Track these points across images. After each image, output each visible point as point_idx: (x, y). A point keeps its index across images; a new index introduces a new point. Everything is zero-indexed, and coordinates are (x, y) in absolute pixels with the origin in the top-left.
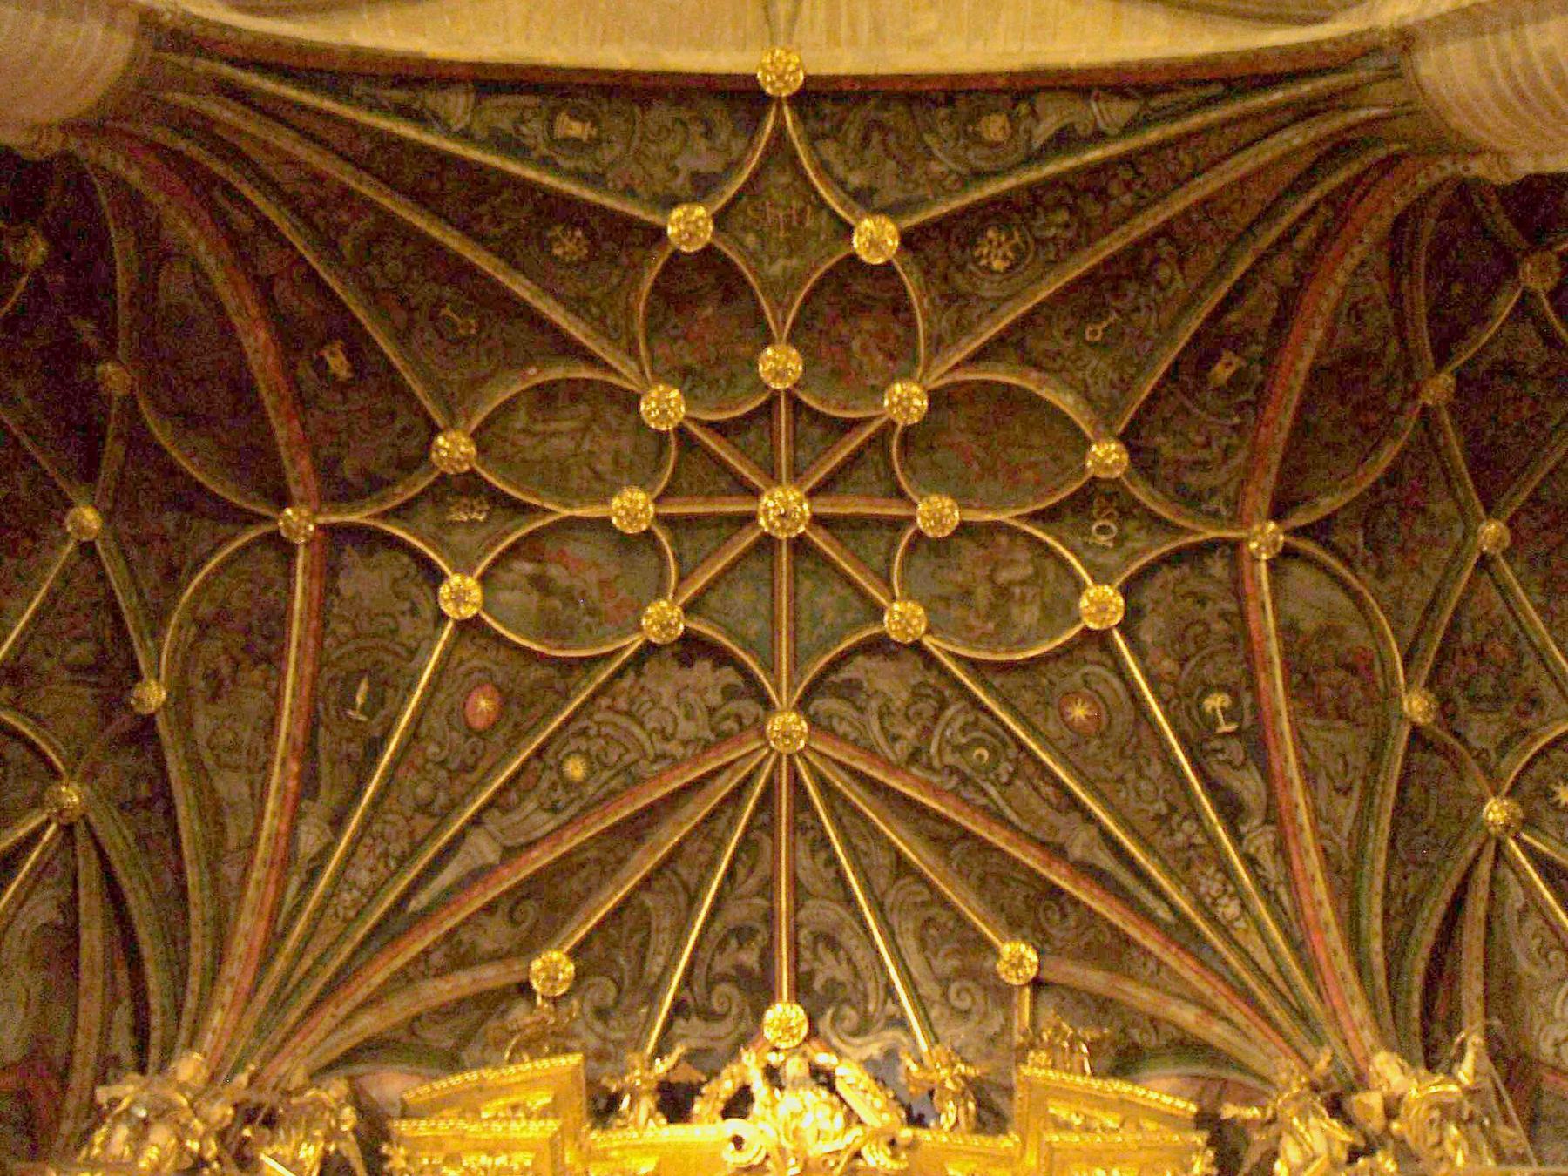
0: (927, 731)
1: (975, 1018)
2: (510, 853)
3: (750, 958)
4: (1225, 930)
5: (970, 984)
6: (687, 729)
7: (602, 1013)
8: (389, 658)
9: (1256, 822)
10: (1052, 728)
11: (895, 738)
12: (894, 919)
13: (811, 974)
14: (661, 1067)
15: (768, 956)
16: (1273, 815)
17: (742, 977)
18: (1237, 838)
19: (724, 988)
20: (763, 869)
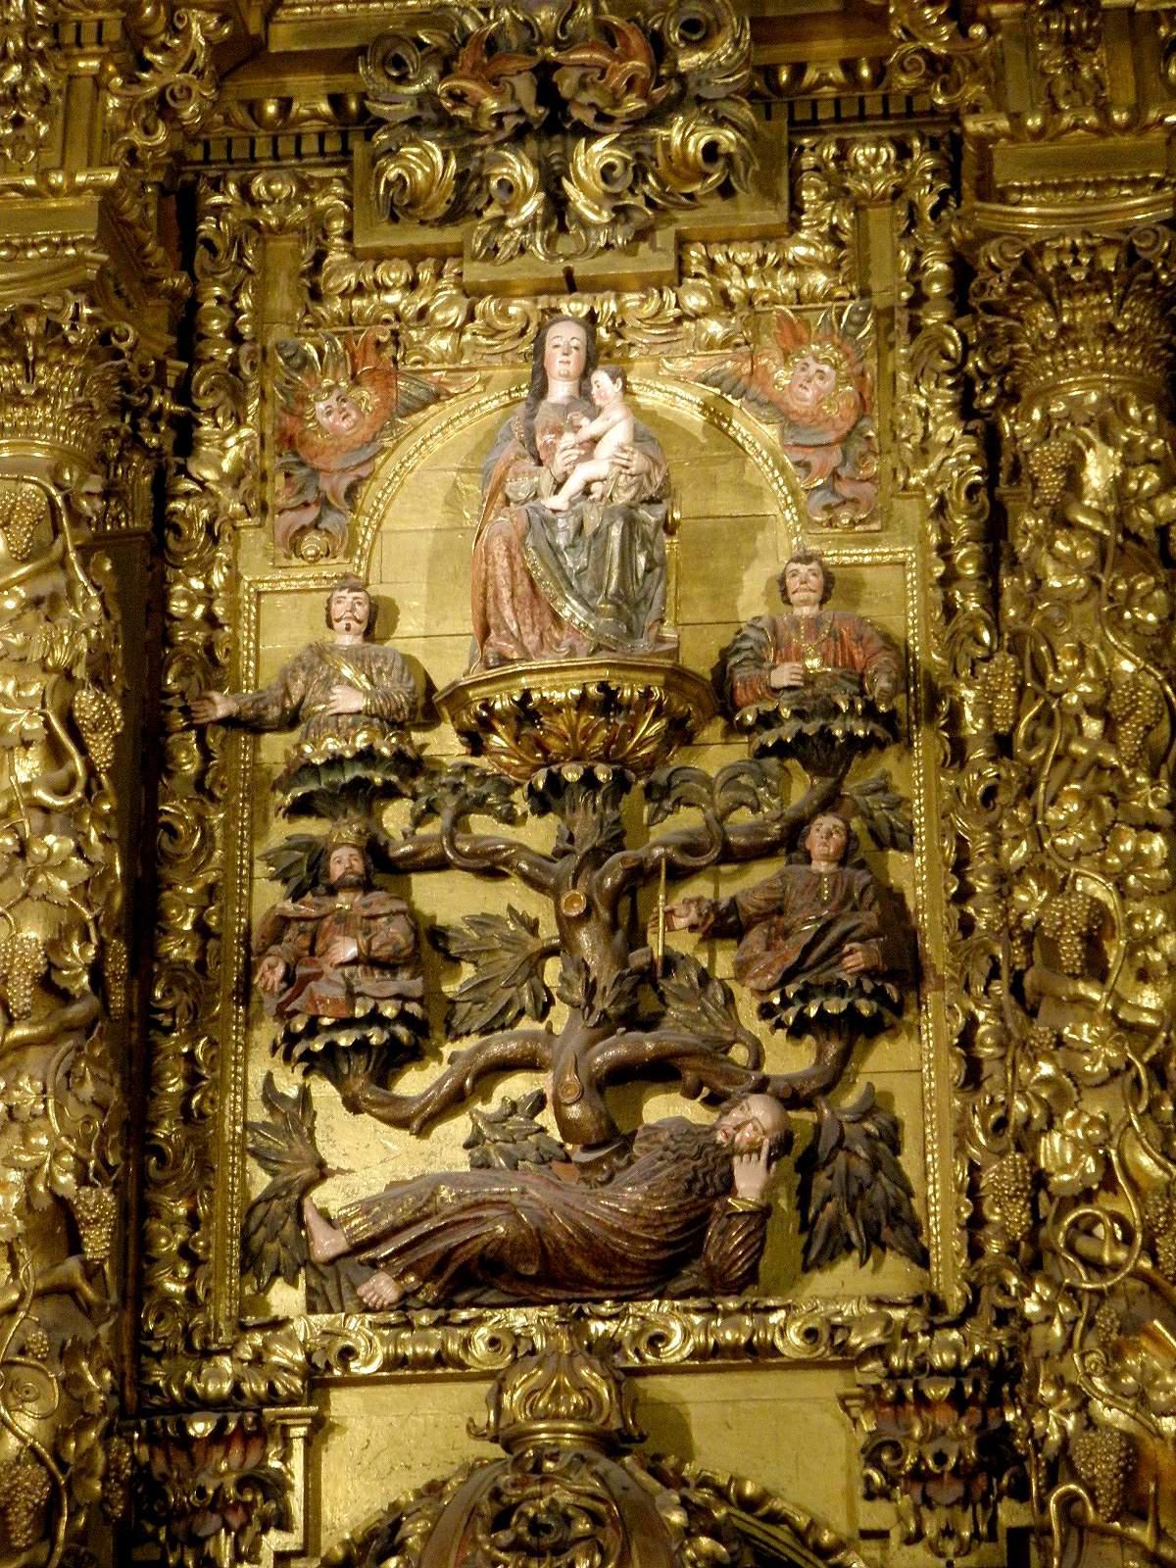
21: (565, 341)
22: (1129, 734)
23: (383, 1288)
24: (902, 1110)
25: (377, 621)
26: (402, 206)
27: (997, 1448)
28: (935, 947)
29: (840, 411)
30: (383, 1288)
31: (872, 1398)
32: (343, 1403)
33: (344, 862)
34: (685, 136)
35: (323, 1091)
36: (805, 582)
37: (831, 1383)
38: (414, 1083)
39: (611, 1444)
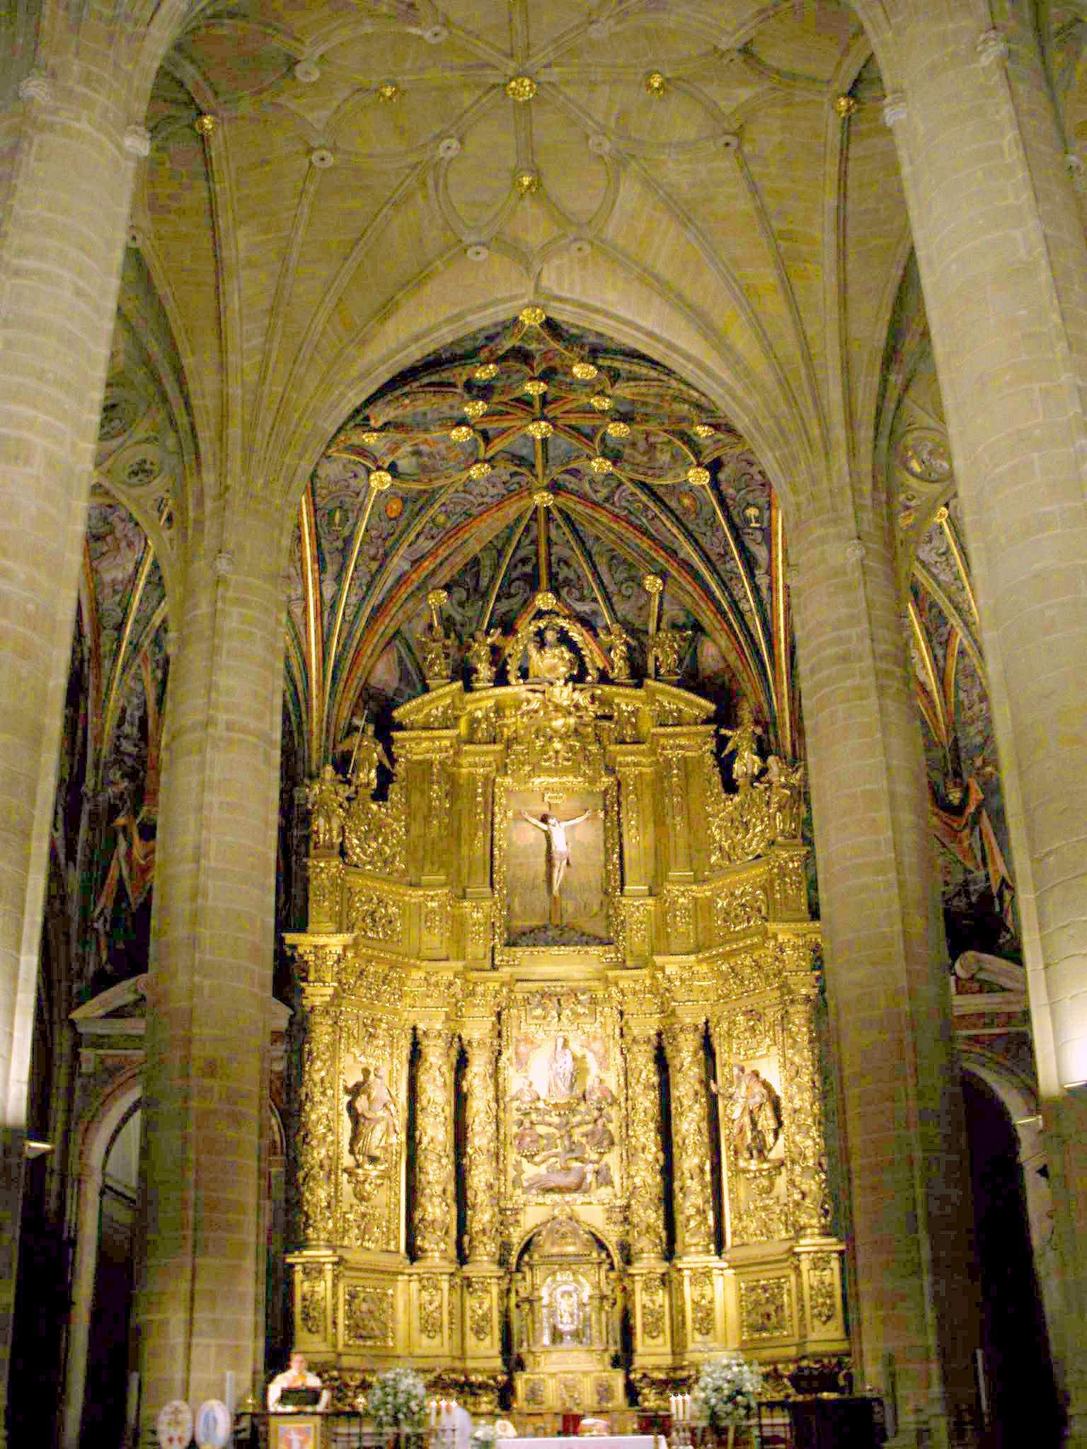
0: (613, 493)
1: (633, 599)
2: (416, 563)
3: (528, 569)
4: (740, 615)
5: (630, 583)
6: (493, 491)
7: (461, 604)
8: (347, 499)
9: (762, 571)
10: (673, 504)
11: (596, 492)
12: (596, 559)
13: (557, 573)
14: (489, 640)
15: (536, 567)
16: (770, 571)
17: (524, 577)
18: (751, 576)
19: (517, 583)
20: (533, 533)
21: (560, 1041)
22: (649, 1116)
23: (534, 1191)
24: (611, 1165)
25: (530, 1085)
26: (537, 1018)
27: (626, 1219)
28: (616, 1140)
29: (602, 1051)
30: (534, 1191)
31: (607, 1210)
32: (528, 1209)
33: (527, 1125)
34: (580, 1010)
35: (524, 1160)
36: (597, 1080)
37: (601, 1207)
38: (537, 1159)
39: (570, 1218)
